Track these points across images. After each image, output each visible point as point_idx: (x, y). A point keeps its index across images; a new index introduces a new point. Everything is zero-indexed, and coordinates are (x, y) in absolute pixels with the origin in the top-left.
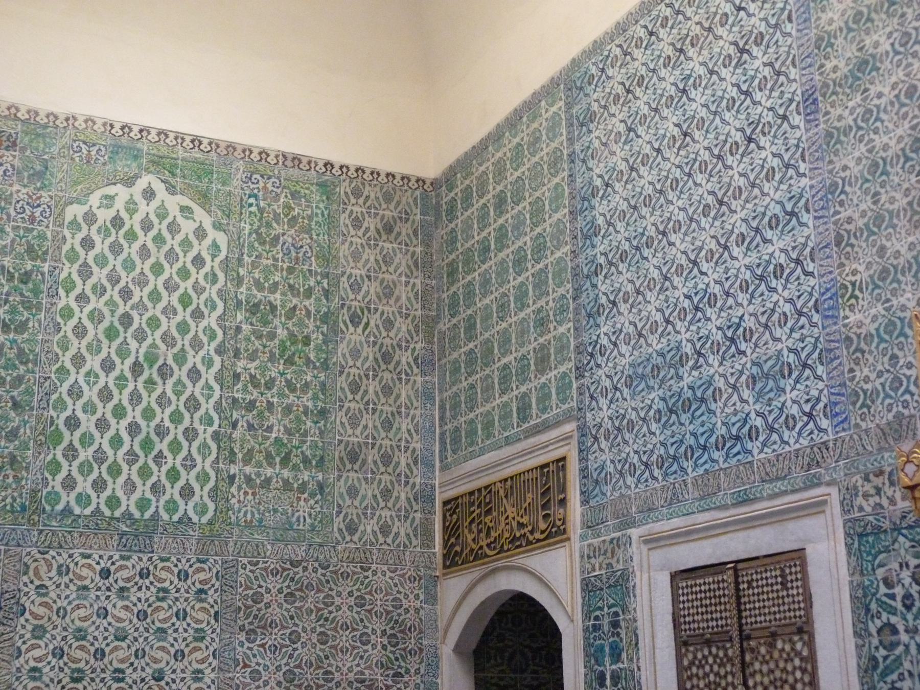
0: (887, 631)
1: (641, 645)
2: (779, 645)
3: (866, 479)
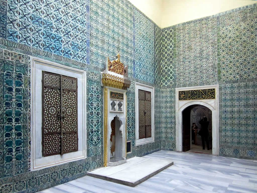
0: (92, 95)
1: (31, 84)
2: (70, 93)
3: (91, 73)
